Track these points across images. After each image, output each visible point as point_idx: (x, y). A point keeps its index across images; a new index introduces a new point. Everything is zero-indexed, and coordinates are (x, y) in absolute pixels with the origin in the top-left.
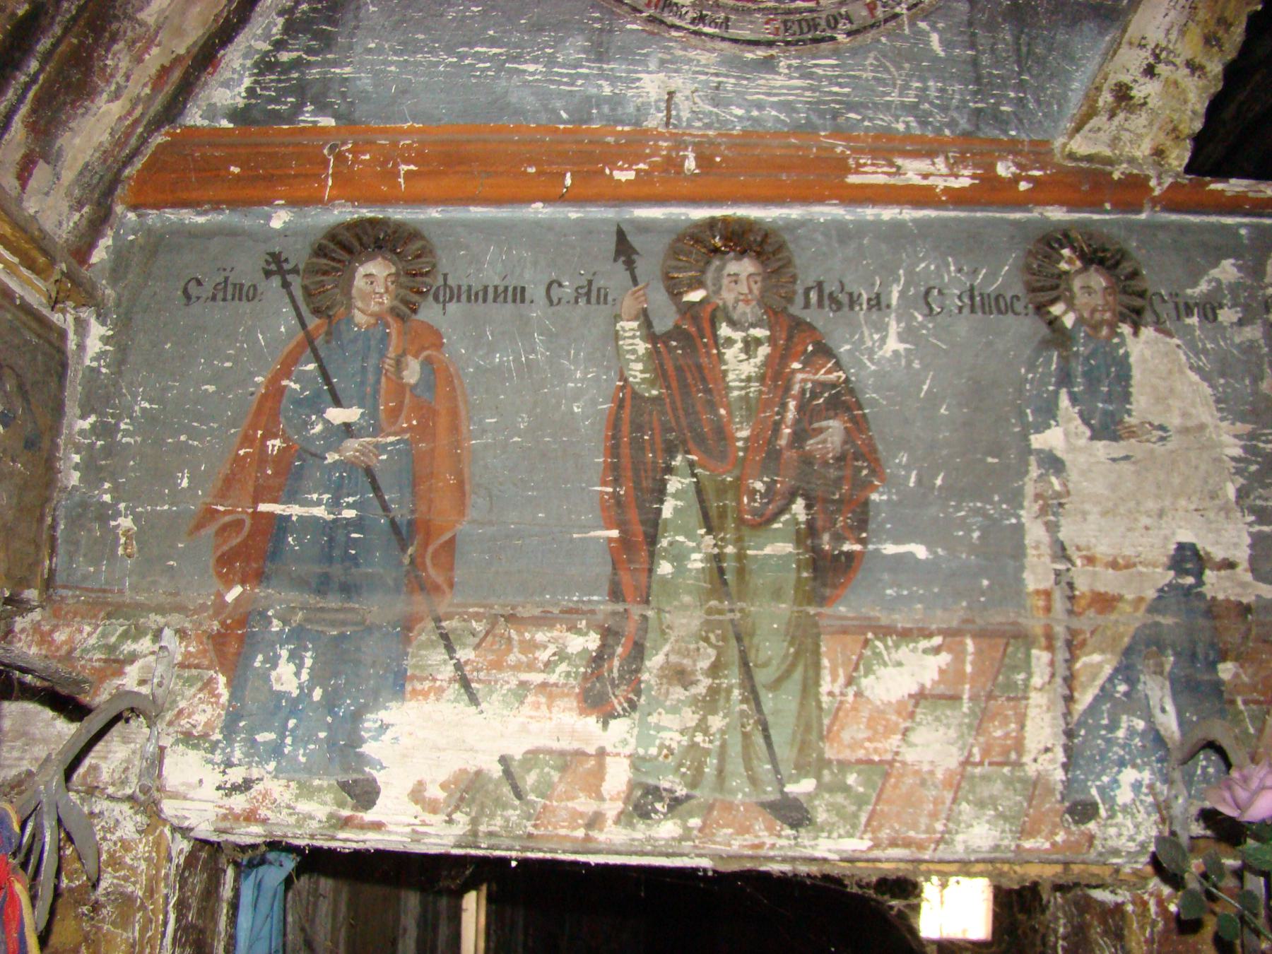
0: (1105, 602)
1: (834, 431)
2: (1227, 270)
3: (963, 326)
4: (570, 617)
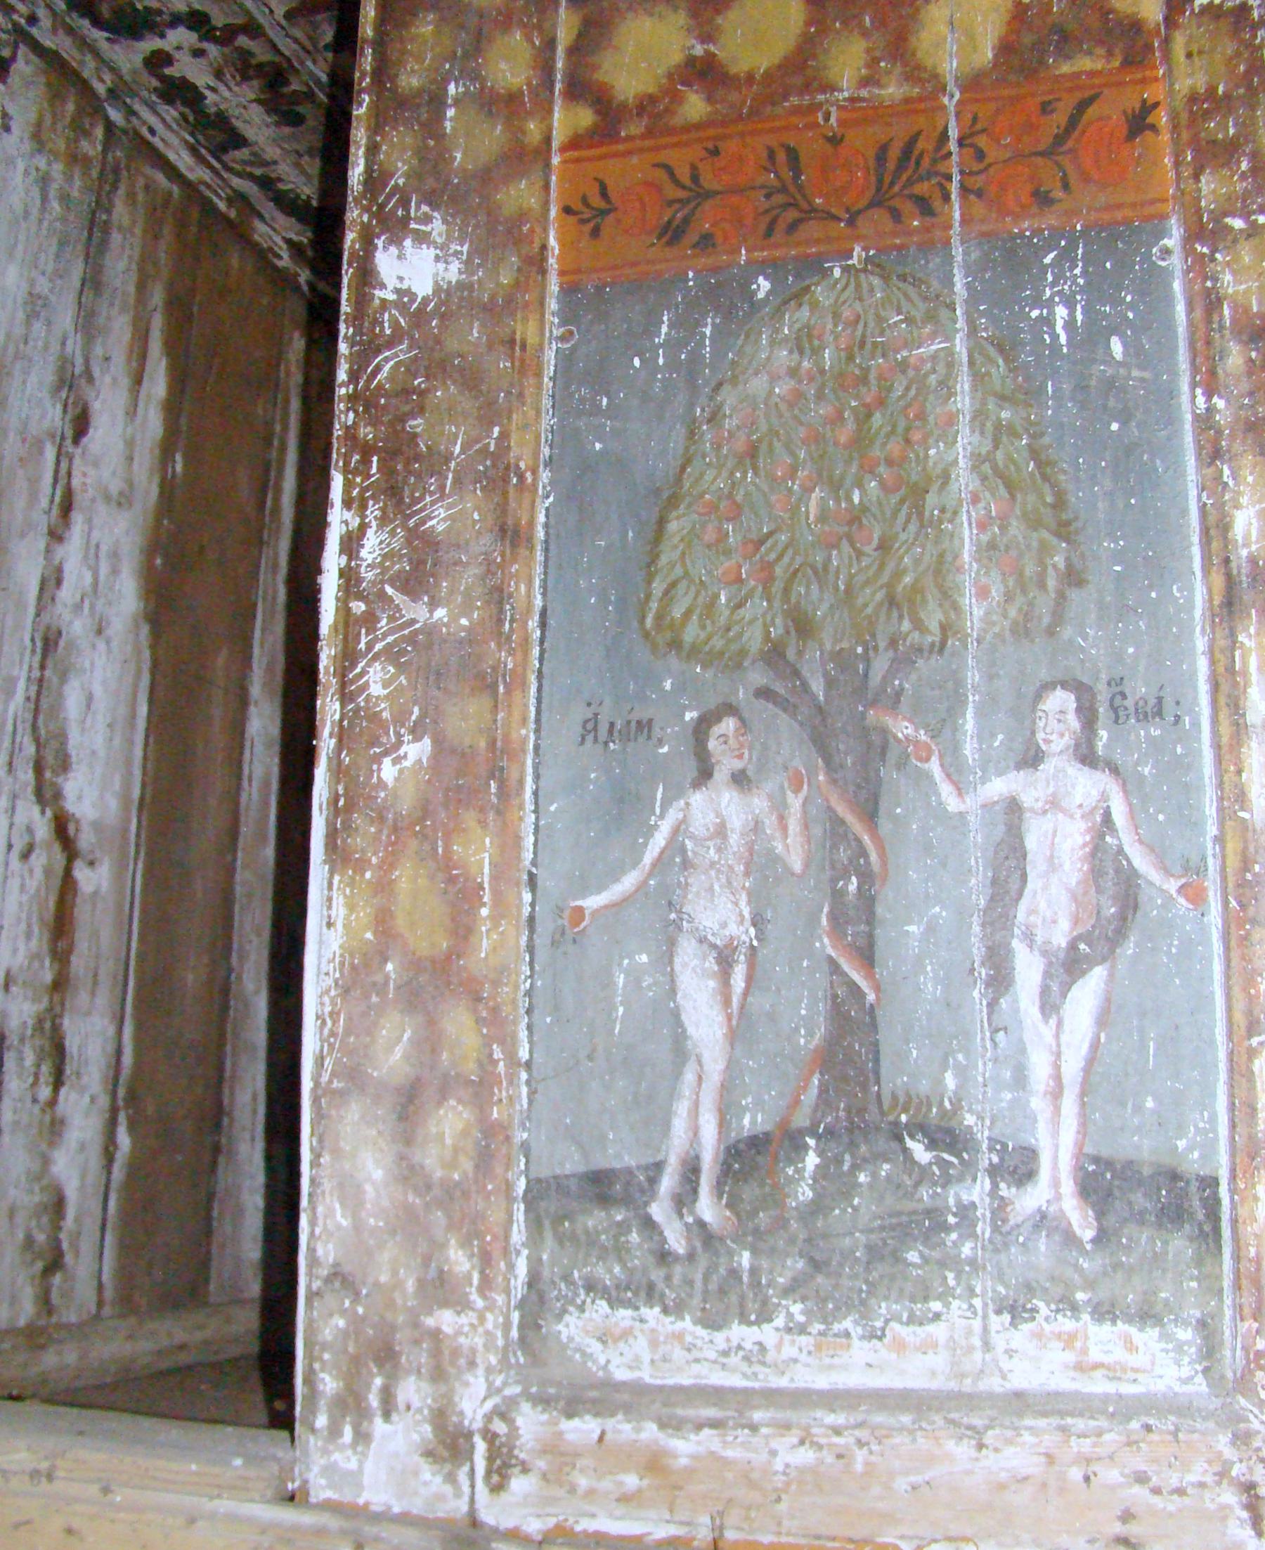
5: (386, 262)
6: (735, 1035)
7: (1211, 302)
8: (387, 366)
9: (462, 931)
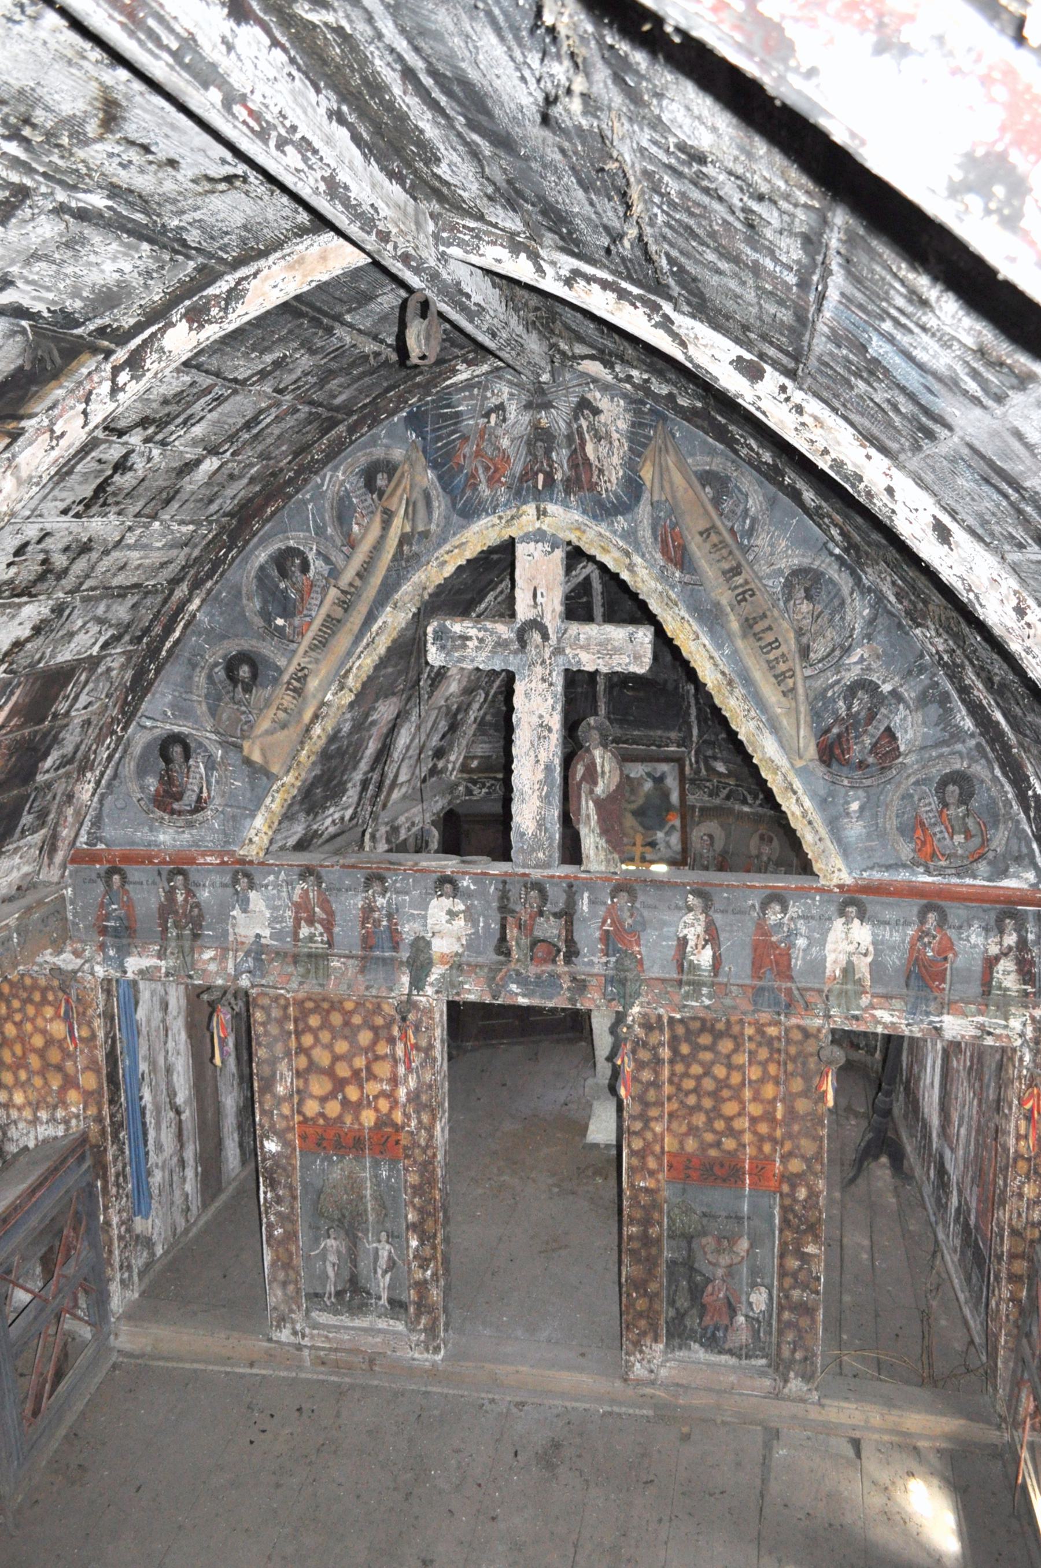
0: (243, 943)
1: (196, 910)
2: (271, 878)
3: (220, 890)
4: (155, 943)
5: (266, 1143)
6: (337, 1275)
7: (406, 1181)
8: (268, 1163)
9: (291, 1259)
